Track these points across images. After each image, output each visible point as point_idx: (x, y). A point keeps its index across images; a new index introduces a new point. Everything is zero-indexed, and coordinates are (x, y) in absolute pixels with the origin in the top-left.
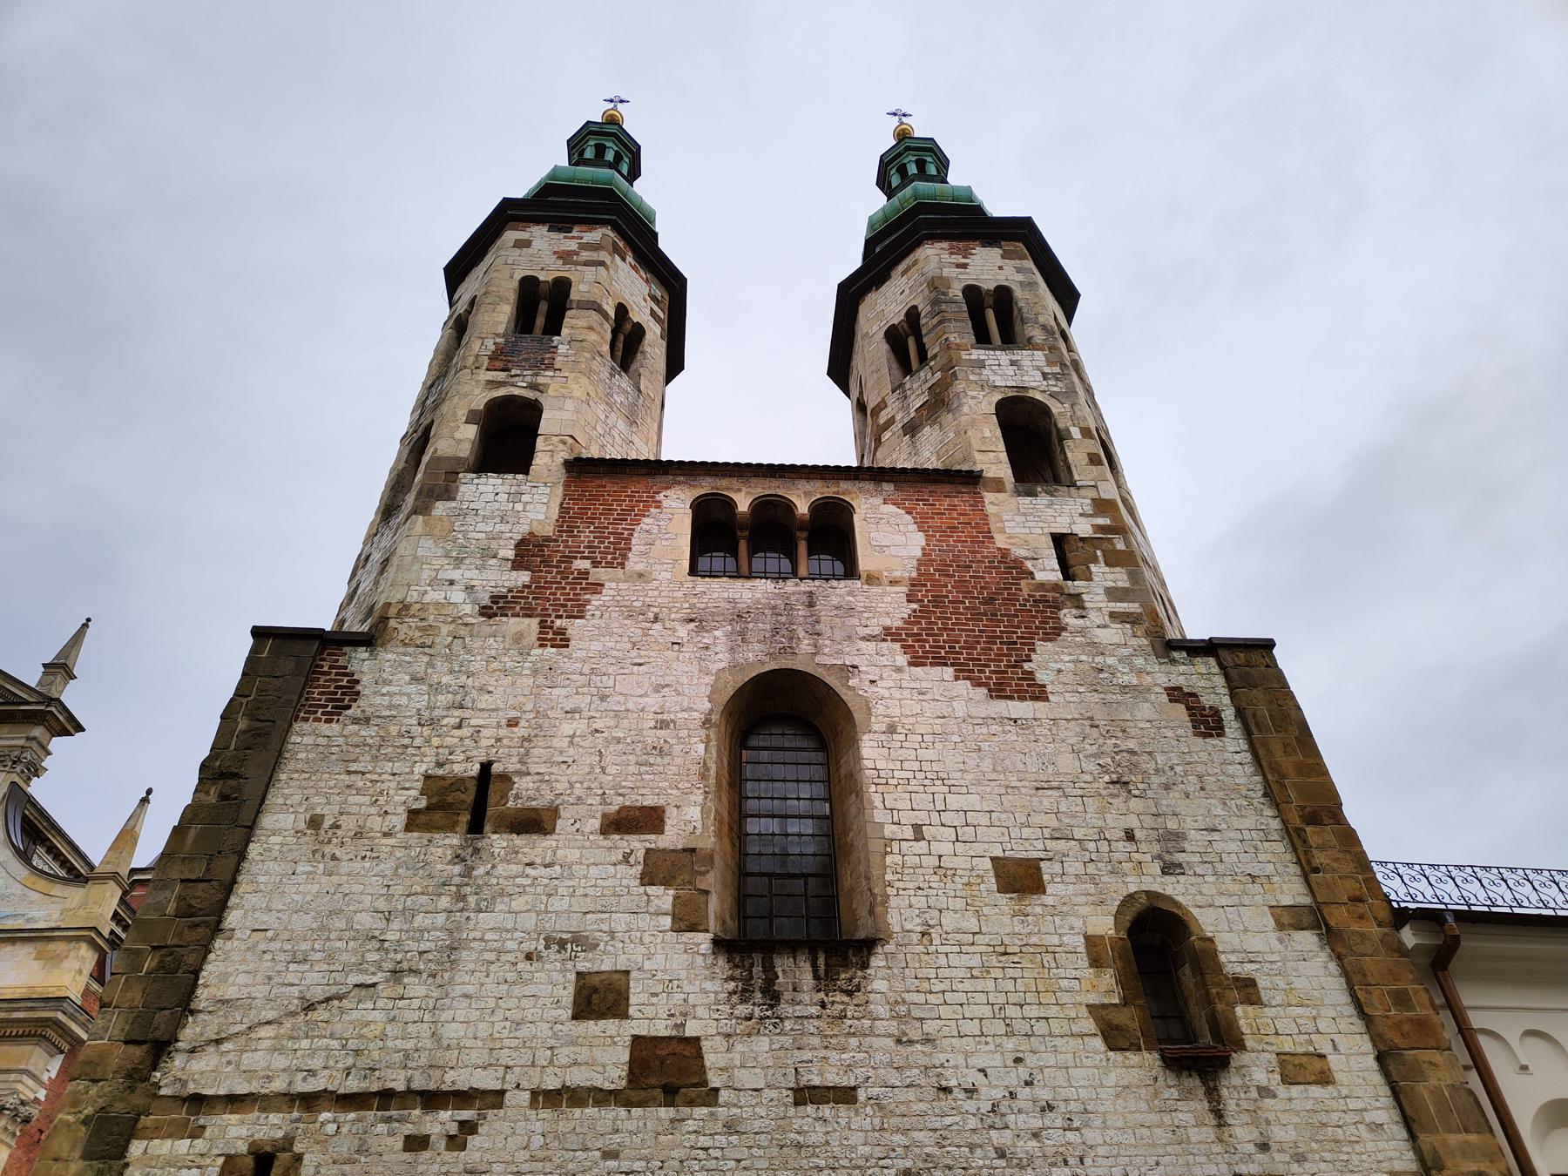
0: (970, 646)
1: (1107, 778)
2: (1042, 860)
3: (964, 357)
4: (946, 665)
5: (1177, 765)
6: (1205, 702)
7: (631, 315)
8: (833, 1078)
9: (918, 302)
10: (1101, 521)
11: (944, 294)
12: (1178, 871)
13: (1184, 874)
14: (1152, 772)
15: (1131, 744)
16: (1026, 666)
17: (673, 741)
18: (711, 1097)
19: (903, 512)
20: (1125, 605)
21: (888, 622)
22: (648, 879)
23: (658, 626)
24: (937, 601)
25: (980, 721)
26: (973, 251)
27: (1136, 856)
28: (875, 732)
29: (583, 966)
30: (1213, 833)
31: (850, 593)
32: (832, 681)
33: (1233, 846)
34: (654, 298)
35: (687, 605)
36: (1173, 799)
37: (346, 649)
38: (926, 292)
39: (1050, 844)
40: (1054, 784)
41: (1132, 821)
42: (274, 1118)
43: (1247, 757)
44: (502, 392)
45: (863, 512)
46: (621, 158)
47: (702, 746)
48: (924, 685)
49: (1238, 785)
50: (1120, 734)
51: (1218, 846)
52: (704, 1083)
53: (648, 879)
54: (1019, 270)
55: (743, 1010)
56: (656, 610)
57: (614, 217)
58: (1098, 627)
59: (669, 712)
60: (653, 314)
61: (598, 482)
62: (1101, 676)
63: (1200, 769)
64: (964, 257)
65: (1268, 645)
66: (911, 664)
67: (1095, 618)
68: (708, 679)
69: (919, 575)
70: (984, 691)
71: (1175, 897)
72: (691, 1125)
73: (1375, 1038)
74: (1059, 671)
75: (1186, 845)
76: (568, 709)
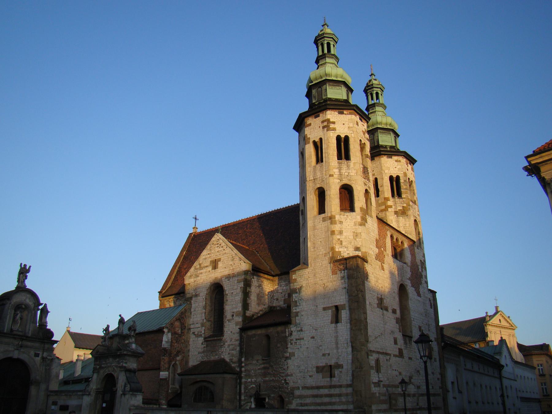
8: (410, 356)
9: (400, 176)
18: (403, 358)
19: (408, 248)
22: (396, 323)
29: (394, 336)
37: (365, 263)
38: (403, 174)
42: (377, 355)
43: (433, 313)
47: (397, 298)
52: (403, 355)
53: (396, 323)
55: (405, 346)
65: (436, 292)
66: (412, 287)
68: (396, 284)
72: (403, 361)
73: (439, 357)
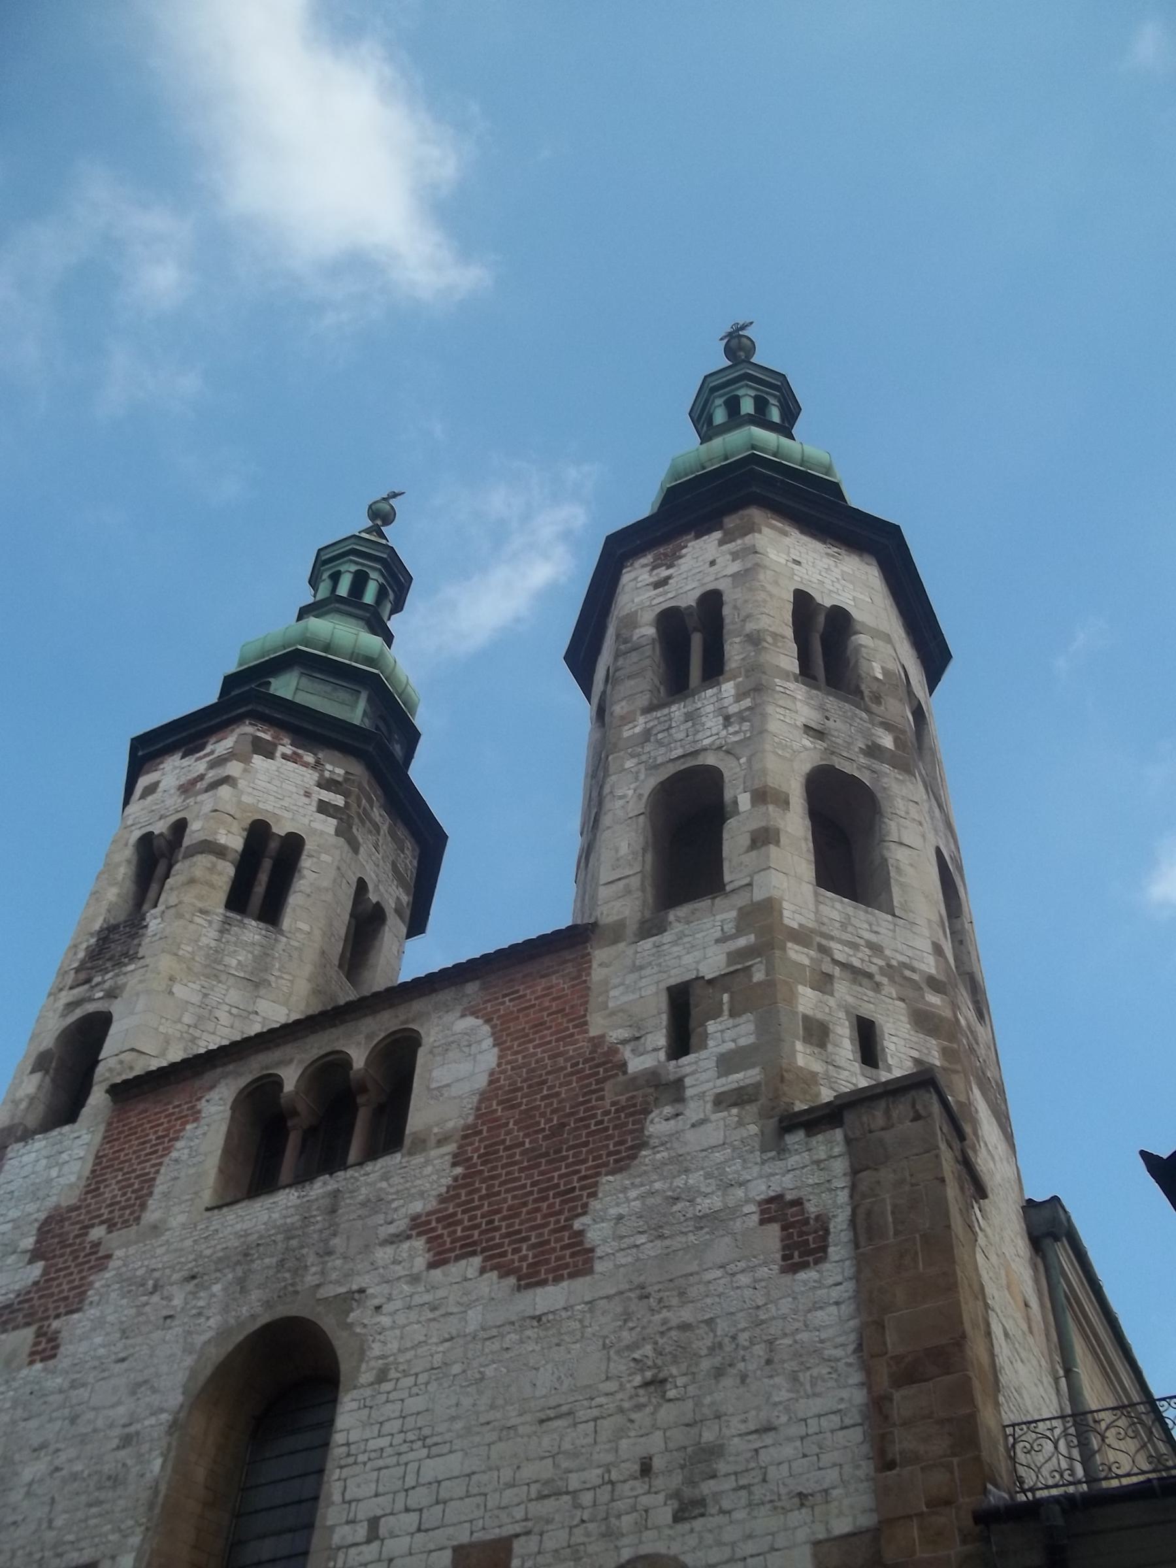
0: (514, 1213)
1: (638, 1380)
2: (517, 1536)
3: (626, 734)
4: (473, 1254)
5: (743, 1330)
6: (812, 1209)
7: (275, 830)
10: (742, 942)
11: (626, 642)
12: (696, 1512)
13: (702, 1515)
14: (704, 1352)
15: (686, 1314)
16: (577, 1225)
17: (129, 1462)
19: (480, 1022)
20: (740, 1076)
21: (417, 1207)
23: (155, 1298)
24: (485, 1158)
25: (494, 1332)
26: (684, 551)
27: (645, 1501)
28: (363, 1386)
30: (764, 1436)
31: (385, 1177)
32: (328, 1323)
33: (788, 1451)
34: (327, 784)
35: (191, 1257)
36: (726, 1393)
39: (537, 1509)
40: (564, 1409)
41: (655, 1443)
44: (78, 1013)
45: (432, 1039)
46: (766, 402)
48: (441, 1293)
49: (822, 1341)
50: (675, 1301)
51: (764, 1457)
54: (735, 556)
56: (157, 1274)
57: (250, 707)
58: (693, 1126)
59: (138, 1421)
60: (324, 808)
61: (141, 1107)
62: (675, 1208)
63: (774, 1329)
64: (669, 567)
67: (693, 1111)
68: (189, 1361)
69: (477, 1117)
70: (512, 1280)
71: (683, 1558)
74: (620, 1217)
75: (722, 1467)
76: (36, 1445)
